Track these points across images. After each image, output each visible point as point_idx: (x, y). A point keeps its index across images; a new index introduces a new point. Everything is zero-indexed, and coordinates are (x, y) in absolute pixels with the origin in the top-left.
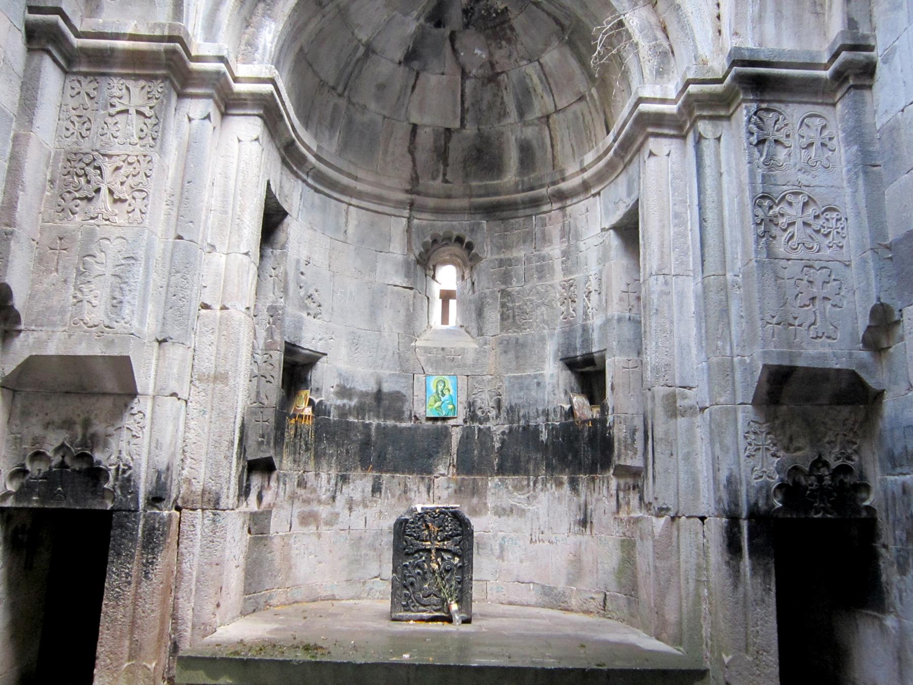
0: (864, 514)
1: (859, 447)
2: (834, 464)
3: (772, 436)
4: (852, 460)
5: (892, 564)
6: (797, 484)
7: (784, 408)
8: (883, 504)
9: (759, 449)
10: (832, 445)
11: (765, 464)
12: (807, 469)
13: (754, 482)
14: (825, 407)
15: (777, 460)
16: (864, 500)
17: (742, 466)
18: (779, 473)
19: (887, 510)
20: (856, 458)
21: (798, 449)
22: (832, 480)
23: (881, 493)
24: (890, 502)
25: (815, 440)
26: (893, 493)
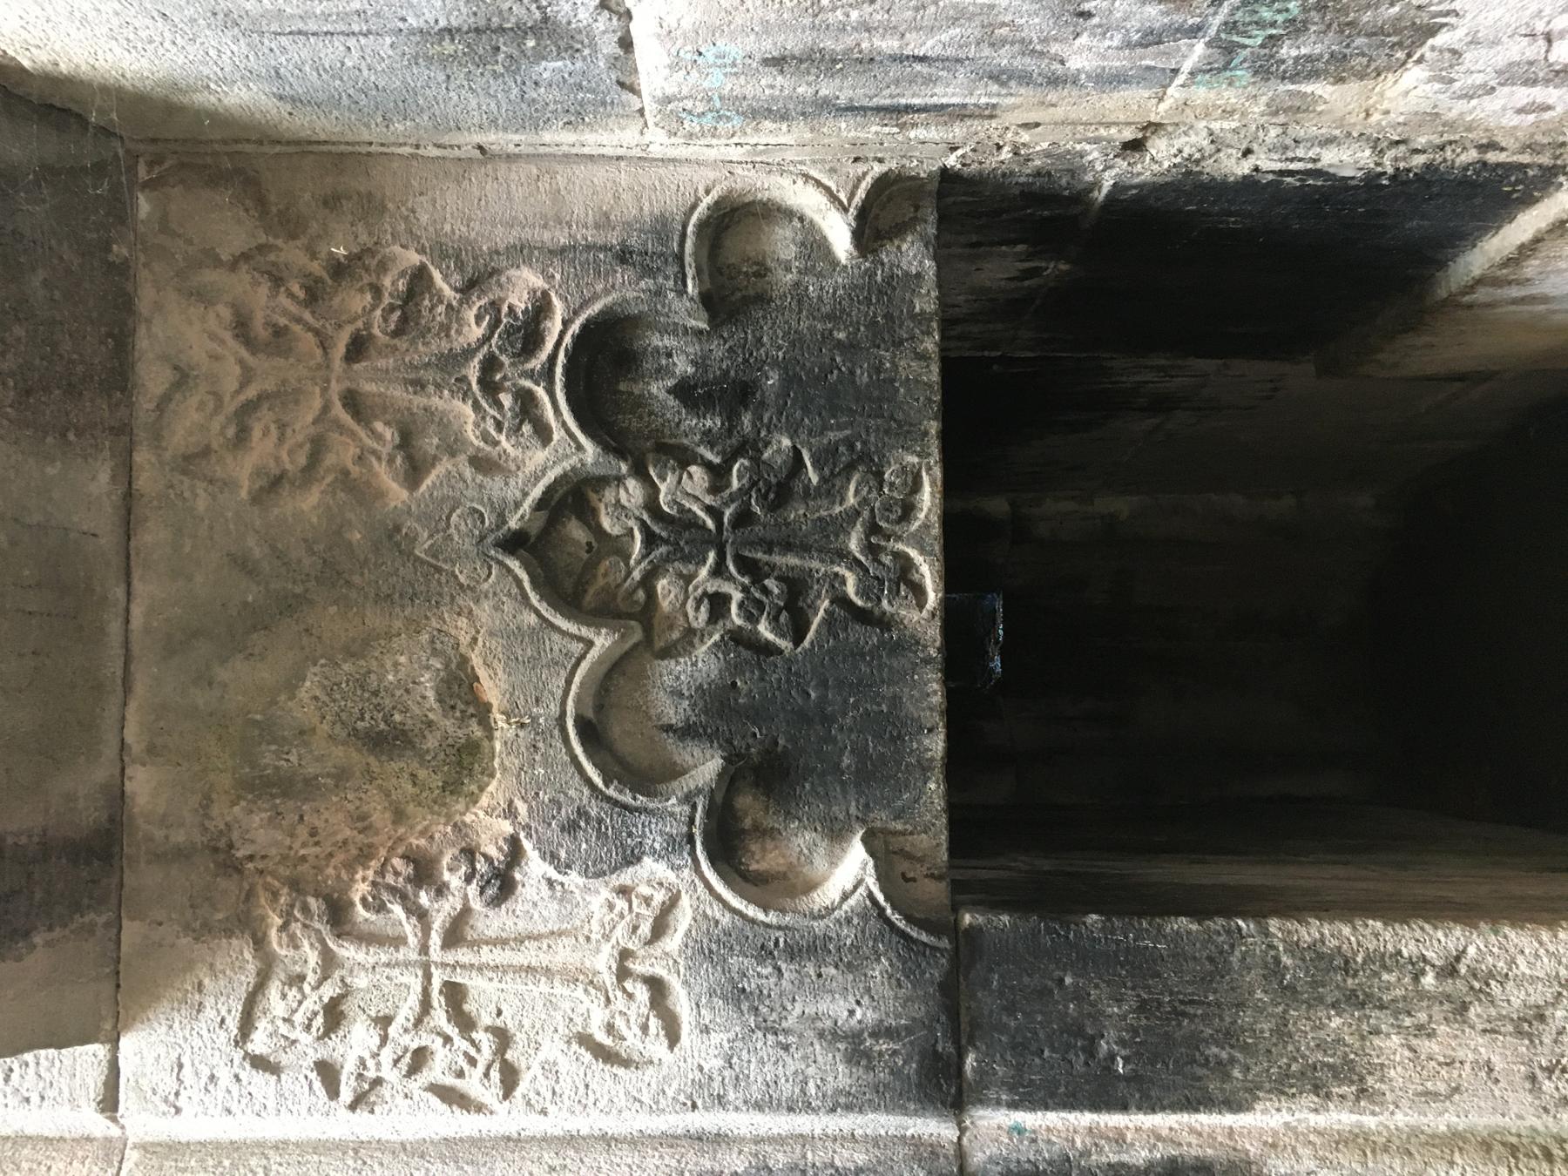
0: (912, 255)
1: (440, 252)
2: (567, 448)
3: (360, 889)
4: (541, 308)
5: (1300, 108)
6: (716, 714)
7: (142, 784)
8: (846, 129)
9: (455, 994)
10: (430, 443)
11: (564, 954)
12: (603, 641)
13: (705, 1045)
14: (145, 481)
15: (535, 867)
16: (815, 245)
17: (583, 1124)
18: (632, 858)
19: (895, 112)
20: (521, 286)
21: (460, 688)
22: (684, 459)
23: (771, 133)
24: (841, 89)
25: (384, 571)
26: (777, 62)
